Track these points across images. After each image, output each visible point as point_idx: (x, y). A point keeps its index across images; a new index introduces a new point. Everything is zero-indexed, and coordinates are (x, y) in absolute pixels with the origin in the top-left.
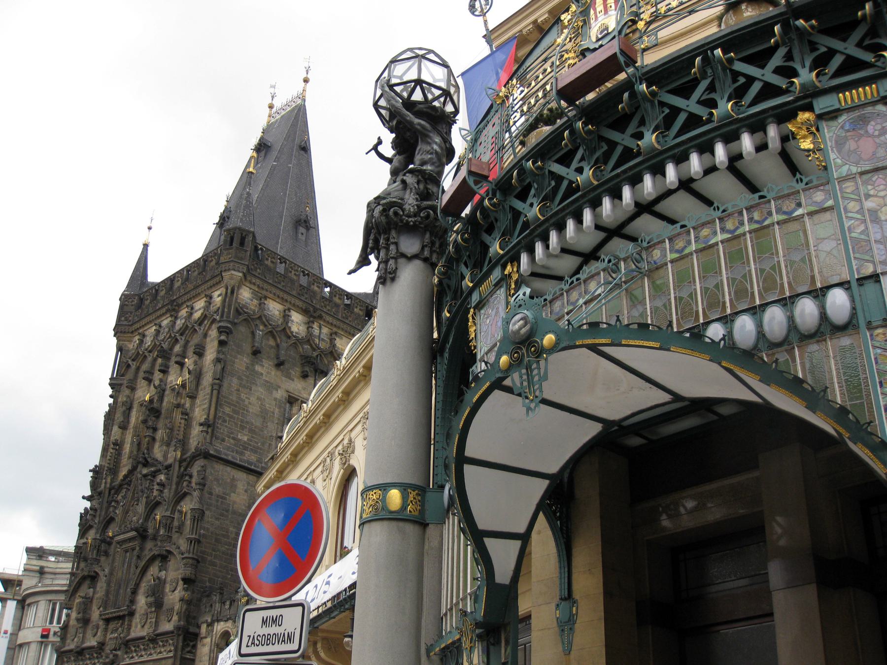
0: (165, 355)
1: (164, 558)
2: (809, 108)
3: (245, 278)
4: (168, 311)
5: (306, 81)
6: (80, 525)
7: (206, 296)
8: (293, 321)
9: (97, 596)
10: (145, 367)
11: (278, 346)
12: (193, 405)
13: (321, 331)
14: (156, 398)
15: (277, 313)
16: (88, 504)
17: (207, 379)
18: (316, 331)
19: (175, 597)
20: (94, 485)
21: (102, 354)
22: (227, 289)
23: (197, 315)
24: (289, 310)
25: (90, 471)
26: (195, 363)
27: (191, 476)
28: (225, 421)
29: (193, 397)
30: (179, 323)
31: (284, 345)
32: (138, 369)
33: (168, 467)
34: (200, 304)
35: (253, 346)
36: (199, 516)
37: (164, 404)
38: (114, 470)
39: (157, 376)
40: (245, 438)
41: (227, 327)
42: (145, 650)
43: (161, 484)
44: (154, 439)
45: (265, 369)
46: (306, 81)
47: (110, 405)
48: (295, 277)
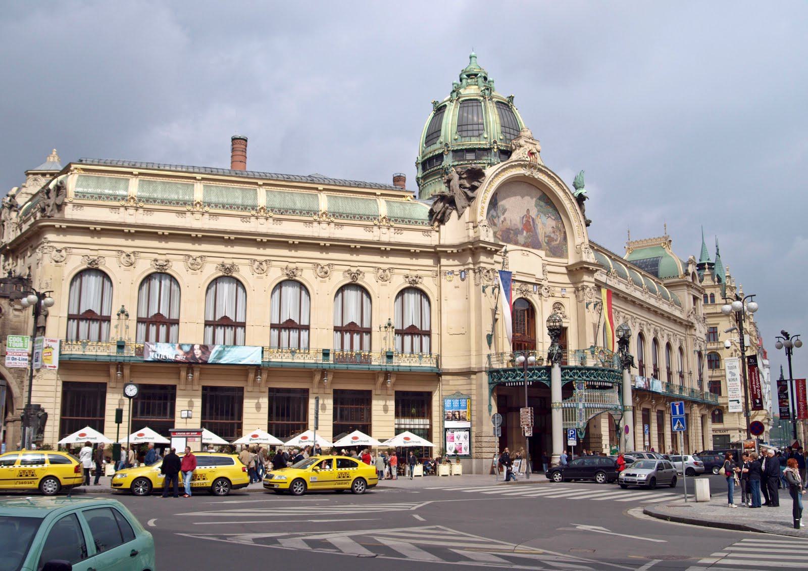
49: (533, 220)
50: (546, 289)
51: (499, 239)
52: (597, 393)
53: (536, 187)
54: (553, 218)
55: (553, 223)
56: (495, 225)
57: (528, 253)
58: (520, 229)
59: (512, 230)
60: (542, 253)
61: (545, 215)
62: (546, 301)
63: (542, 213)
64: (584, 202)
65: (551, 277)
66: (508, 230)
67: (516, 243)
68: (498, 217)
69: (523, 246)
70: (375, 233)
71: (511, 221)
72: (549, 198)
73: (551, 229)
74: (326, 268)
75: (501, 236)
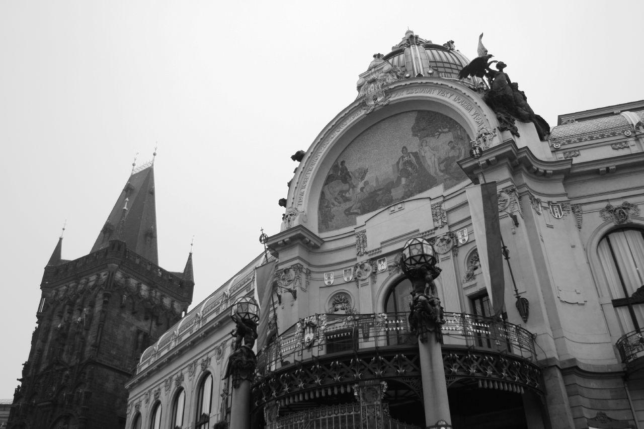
0: (72, 304)
2: (357, 383)
3: (120, 268)
6: (14, 395)
7: (97, 274)
8: (142, 289)
11: (134, 303)
12: (87, 334)
14: (65, 327)
16: (20, 383)
17: (96, 321)
18: (154, 295)
20: (25, 372)
21: (34, 298)
22: (110, 273)
23: (91, 284)
24: (141, 284)
25: (23, 365)
26: (90, 311)
27: (85, 373)
28: (105, 344)
29: (87, 330)
30: (80, 287)
31: (137, 302)
32: (54, 309)
33: (72, 368)
34: (93, 278)
35: (121, 304)
36: (88, 395)
37: (70, 331)
38: (37, 365)
39: (66, 315)
40: (115, 353)
41: (109, 294)
43: (67, 377)
44: (63, 350)
45: (127, 315)
47: (36, 328)
48: (144, 266)
49: (416, 155)
50: (442, 240)
51: (357, 214)
53: (403, 113)
54: (446, 130)
55: (449, 137)
56: (347, 200)
57: (400, 206)
58: (395, 180)
59: (380, 190)
60: (437, 191)
61: (433, 136)
62: (448, 258)
63: (427, 136)
64: (505, 70)
65: (455, 218)
66: (373, 194)
67: (389, 203)
68: (354, 187)
69: (403, 198)
71: (377, 179)
72: (429, 112)
73: (448, 147)
74: (221, 348)
75: (359, 208)
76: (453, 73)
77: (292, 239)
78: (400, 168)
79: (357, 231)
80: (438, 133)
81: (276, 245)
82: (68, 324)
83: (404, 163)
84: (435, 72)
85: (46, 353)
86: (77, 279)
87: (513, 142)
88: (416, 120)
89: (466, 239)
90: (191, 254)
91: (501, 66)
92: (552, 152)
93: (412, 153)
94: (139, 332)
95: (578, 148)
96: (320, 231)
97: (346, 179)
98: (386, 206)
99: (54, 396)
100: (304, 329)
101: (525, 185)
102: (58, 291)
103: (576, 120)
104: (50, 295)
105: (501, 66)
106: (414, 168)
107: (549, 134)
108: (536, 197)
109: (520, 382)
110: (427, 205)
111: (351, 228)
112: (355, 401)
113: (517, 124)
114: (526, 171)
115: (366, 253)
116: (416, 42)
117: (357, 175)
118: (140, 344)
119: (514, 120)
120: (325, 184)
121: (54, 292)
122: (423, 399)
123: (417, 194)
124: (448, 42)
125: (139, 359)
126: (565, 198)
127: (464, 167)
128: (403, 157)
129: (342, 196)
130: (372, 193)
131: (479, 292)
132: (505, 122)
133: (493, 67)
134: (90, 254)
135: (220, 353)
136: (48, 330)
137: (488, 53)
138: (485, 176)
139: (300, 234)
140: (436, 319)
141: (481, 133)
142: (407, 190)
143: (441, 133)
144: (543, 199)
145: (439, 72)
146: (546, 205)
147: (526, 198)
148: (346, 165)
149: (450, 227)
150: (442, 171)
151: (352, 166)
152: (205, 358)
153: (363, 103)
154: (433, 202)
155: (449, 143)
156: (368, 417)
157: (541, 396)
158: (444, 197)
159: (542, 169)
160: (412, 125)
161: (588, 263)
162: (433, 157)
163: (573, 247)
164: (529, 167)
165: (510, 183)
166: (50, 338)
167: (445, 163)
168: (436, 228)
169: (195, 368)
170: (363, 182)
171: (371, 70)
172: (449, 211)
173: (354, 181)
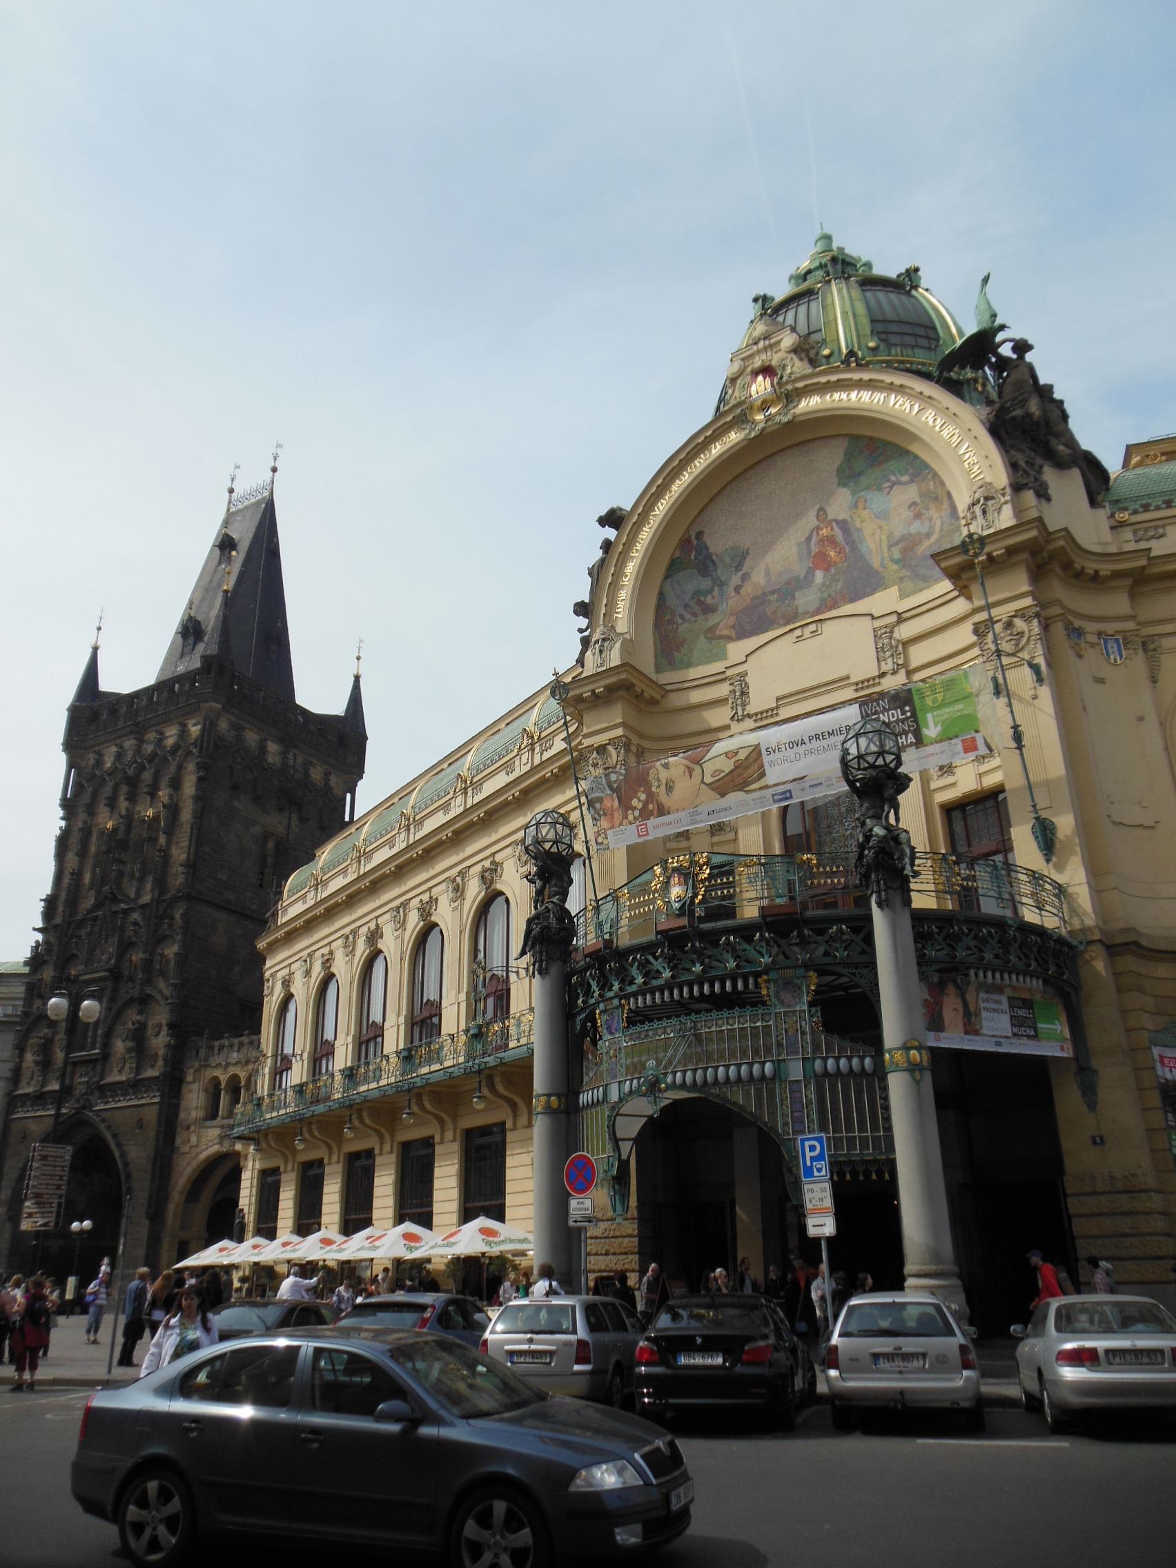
0: (133, 782)
1: (144, 1002)
2: (767, 974)
4: (131, 732)
5: (274, 470)
7: (180, 724)
9: (58, 1037)
10: (107, 791)
13: (297, 759)
14: (122, 827)
15: (253, 744)
17: (186, 815)
18: (291, 762)
19: (160, 1042)
23: (170, 742)
24: (266, 740)
26: (171, 797)
27: (172, 918)
33: (143, 907)
36: (182, 959)
37: (132, 835)
39: (123, 805)
40: (225, 878)
42: (123, 1095)
46: (274, 470)
49: (843, 524)
51: (729, 639)
52: (668, 1031)
53: (821, 438)
54: (906, 478)
55: (911, 493)
57: (812, 627)
58: (802, 576)
59: (773, 592)
60: (885, 601)
61: (879, 489)
63: (867, 488)
64: (1029, 357)
66: (760, 600)
68: (722, 585)
70: (517, 769)
72: (871, 439)
73: (908, 514)
74: (459, 880)
75: (733, 627)
76: (917, 346)
77: (610, 689)
78: (813, 547)
79: (729, 673)
80: (888, 484)
81: (580, 699)
82: (129, 820)
83: (820, 541)
84: (882, 346)
85: (87, 878)
86: (139, 732)
87: (1040, 520)
88: (846, 454)
89: (940, 697)
90: (357, 678)
91: (1022, 347)
92: (1112, 528)
93: (837, 522)
94: (266, 836)
95: (1160, 523)
96: (659, 669)
97: (706, 567)
98: (785, 625)
99: (113, 961)
100: (669, 878)
101: (1058, 602)
102: (100, 755)
103: (1163, 454)
104: (83, 764)
105: (1022, 347)
106: (840, 553)
107: (1108, 489)
108: (1077, 623)
109: (1039, 970)
110: (866, 626)
111: (718, 667)
112: (764, 1004)
113: (1049, 475)
114: (1060, 572)
115: (749, 716)
116: (843, 272)
117: (728, 560)
118: (270, 860)
119: (1041, 467)
120: (667, 577)
121: (91, 758)
122: (879, 1001)
123: (846, 603)
124: (907, 271)
125: (281, 893)
126: (1130, 625)
127: (943, 565)
128: (818, 529)
129: (700, 603)
130: (756, 598)
131: (961, 798)
132: (1025, 472)
133: (1006, 350)
134: (159, 687)
135: (459, 891)
136: (86, 833)
137: (999, 321)
138: (987, 584)
139: (626, 679)
140: (903, 868)
141: (977, 495)
142: (826, 595)
143: (894, 484)
144: (1091, 627)
145: (890, 345)
146: (1093, 639)
147: (1058, 628)
148: (707, 539)
149: (909, 673)
150: (896, 562)
151: (718, 542)
152: (425, 897)
153: (740, 415)
154: (877, 623)
155: (910, 506)
156: (786, 1031)
157: (1072, 992)
158: (899, 614)
159: (1091, 566)
160: (837, 464)
161: (1166, 749)
162: (878, 532)
163: (1141, 719)
164: (1067, 565)
165: (1028, 601)
166: (93, 849)
167: (901, 545)
168: (883, 675)
169: (405, 915)
170: (740, 574)
171: (756, 343)
172: (907, 643)
173: (721, 573)
